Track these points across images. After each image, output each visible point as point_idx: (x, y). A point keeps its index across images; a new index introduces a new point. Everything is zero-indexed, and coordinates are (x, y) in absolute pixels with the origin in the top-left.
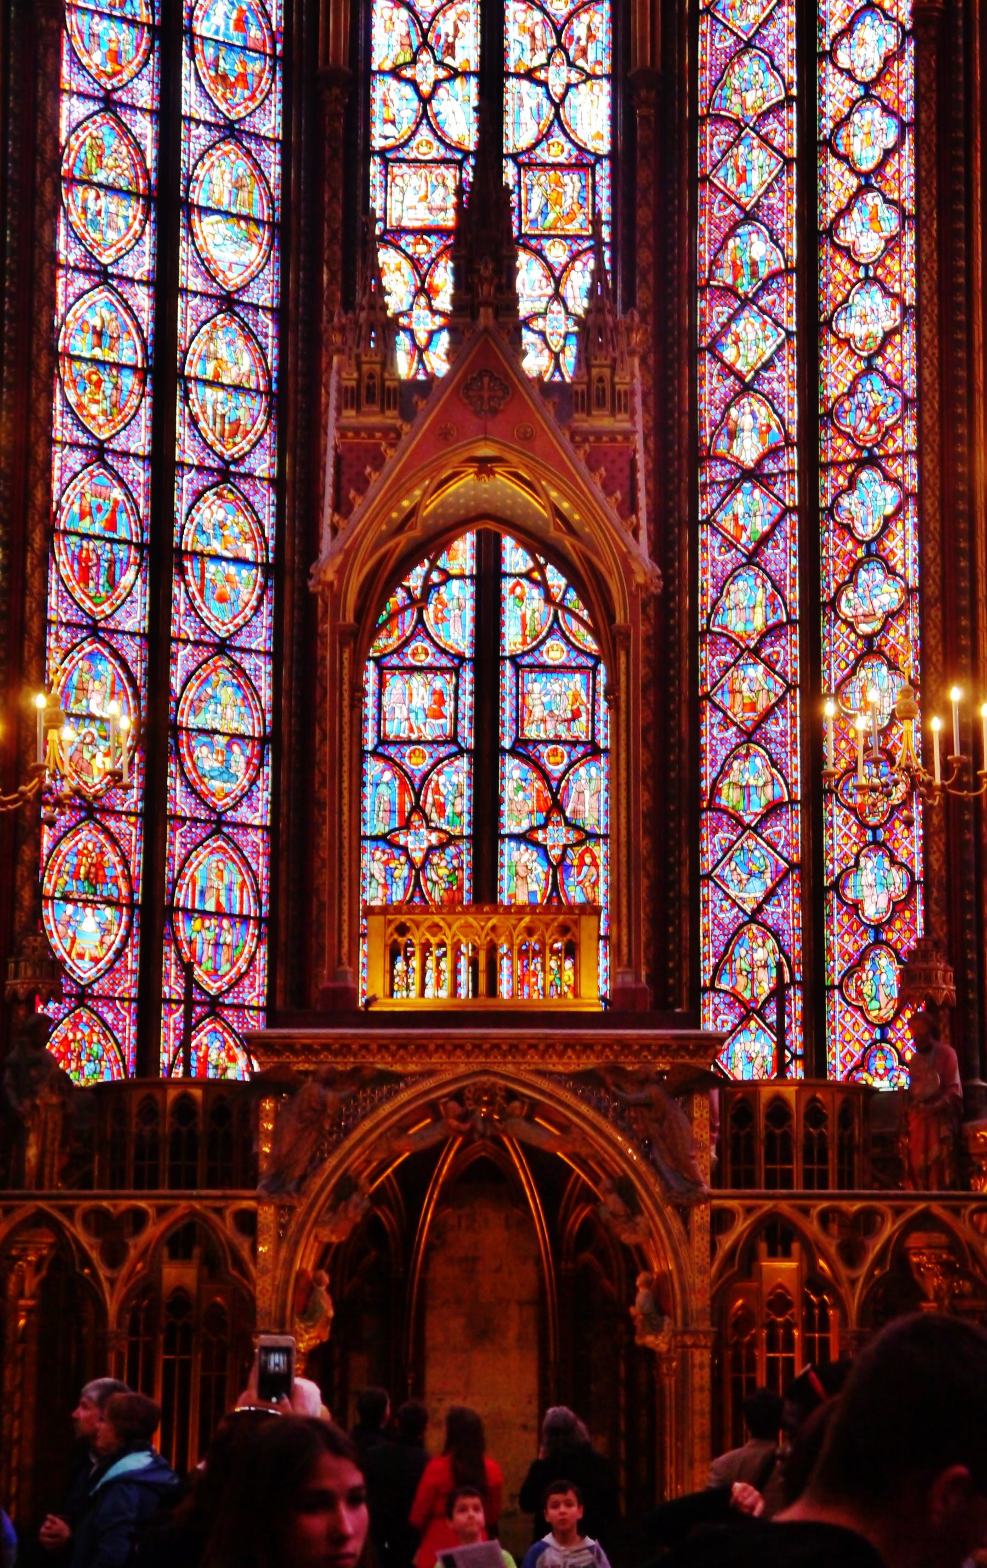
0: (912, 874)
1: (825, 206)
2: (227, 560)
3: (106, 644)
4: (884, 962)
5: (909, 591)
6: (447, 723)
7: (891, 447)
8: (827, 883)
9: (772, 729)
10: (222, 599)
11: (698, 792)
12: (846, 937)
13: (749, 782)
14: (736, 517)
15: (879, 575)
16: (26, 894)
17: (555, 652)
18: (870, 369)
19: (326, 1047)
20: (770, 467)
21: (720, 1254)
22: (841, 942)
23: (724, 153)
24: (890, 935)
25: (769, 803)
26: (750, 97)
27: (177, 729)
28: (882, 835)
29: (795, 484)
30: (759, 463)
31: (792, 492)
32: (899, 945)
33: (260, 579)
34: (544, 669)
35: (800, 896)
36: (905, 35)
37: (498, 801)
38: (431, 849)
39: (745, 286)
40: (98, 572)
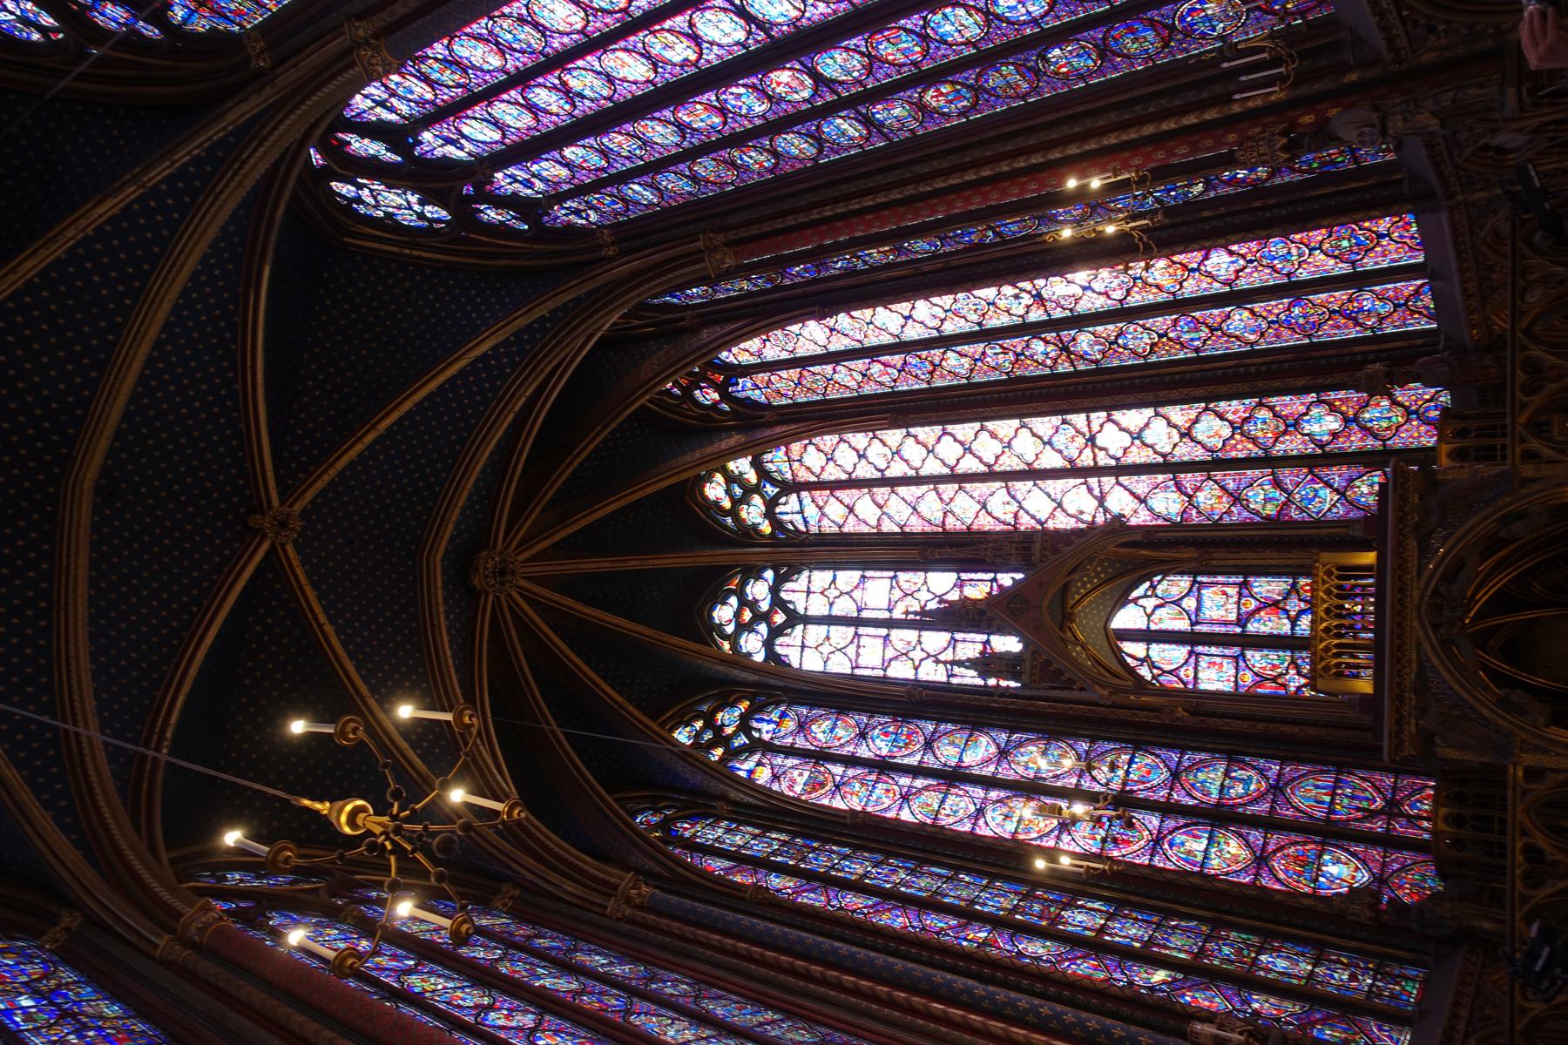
4: (1367, 416)
5: (1157, 414)
6: (1225, 661)
7: (1085, 430)
9: (1231, 486)
10: (1149, 773)
13: (1262, 497)
16: (1306, 902)
17: (1190, 603)
18: (1049, 443)
19: (1398, 710)
20: (1097, 492)
21: (1558, 457)
22: (1356, 442)
27: (1218, 805)
28: (1291, 421)
29: (1103, 479)
34: (1199, 608)
35: (1328, 466)
36: (908, 435)
37: (1271, 635)
38: (1299, 673)
39: (1014, 507)
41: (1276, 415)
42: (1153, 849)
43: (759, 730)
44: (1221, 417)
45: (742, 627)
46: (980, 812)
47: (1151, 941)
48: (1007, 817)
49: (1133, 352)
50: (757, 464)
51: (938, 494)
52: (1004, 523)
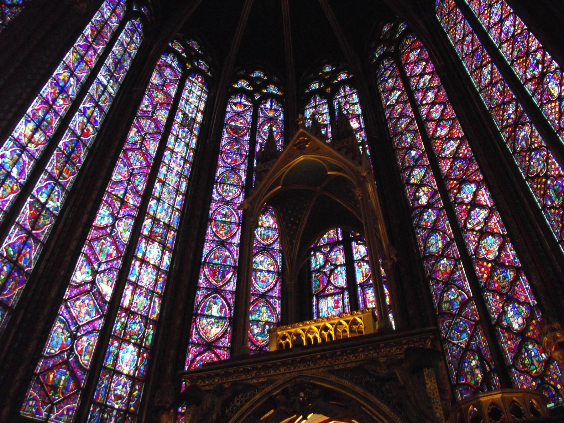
0: (529, 304)
1: (429, 132)
2: (264, 271)
3: (220, 294)
7: (469, 173)
8: (494, 322)
10: (262, 281)
11: (434, 310)
12: (509, 342)
14: (425, 220)
15: (477, 209)
22: (508, 345)
23: (399, 141)
24: (529, 334)
25: (460, 302)
26: (403, 126)
30: (428, 202)
31: (441, 204)
32: (535, 336)
33: (276, 276)
40: (219, 274)
41: (513, 283)
42: (210, 289)
43: (266, 103)
44: (502, 248)
45: (321, 80)
46: (227, 203)
47: (136, 286)
48: (225, 216)
49: (529, 167)
50: (404, 35)
51: (410, 123)
52: (403, 163)
